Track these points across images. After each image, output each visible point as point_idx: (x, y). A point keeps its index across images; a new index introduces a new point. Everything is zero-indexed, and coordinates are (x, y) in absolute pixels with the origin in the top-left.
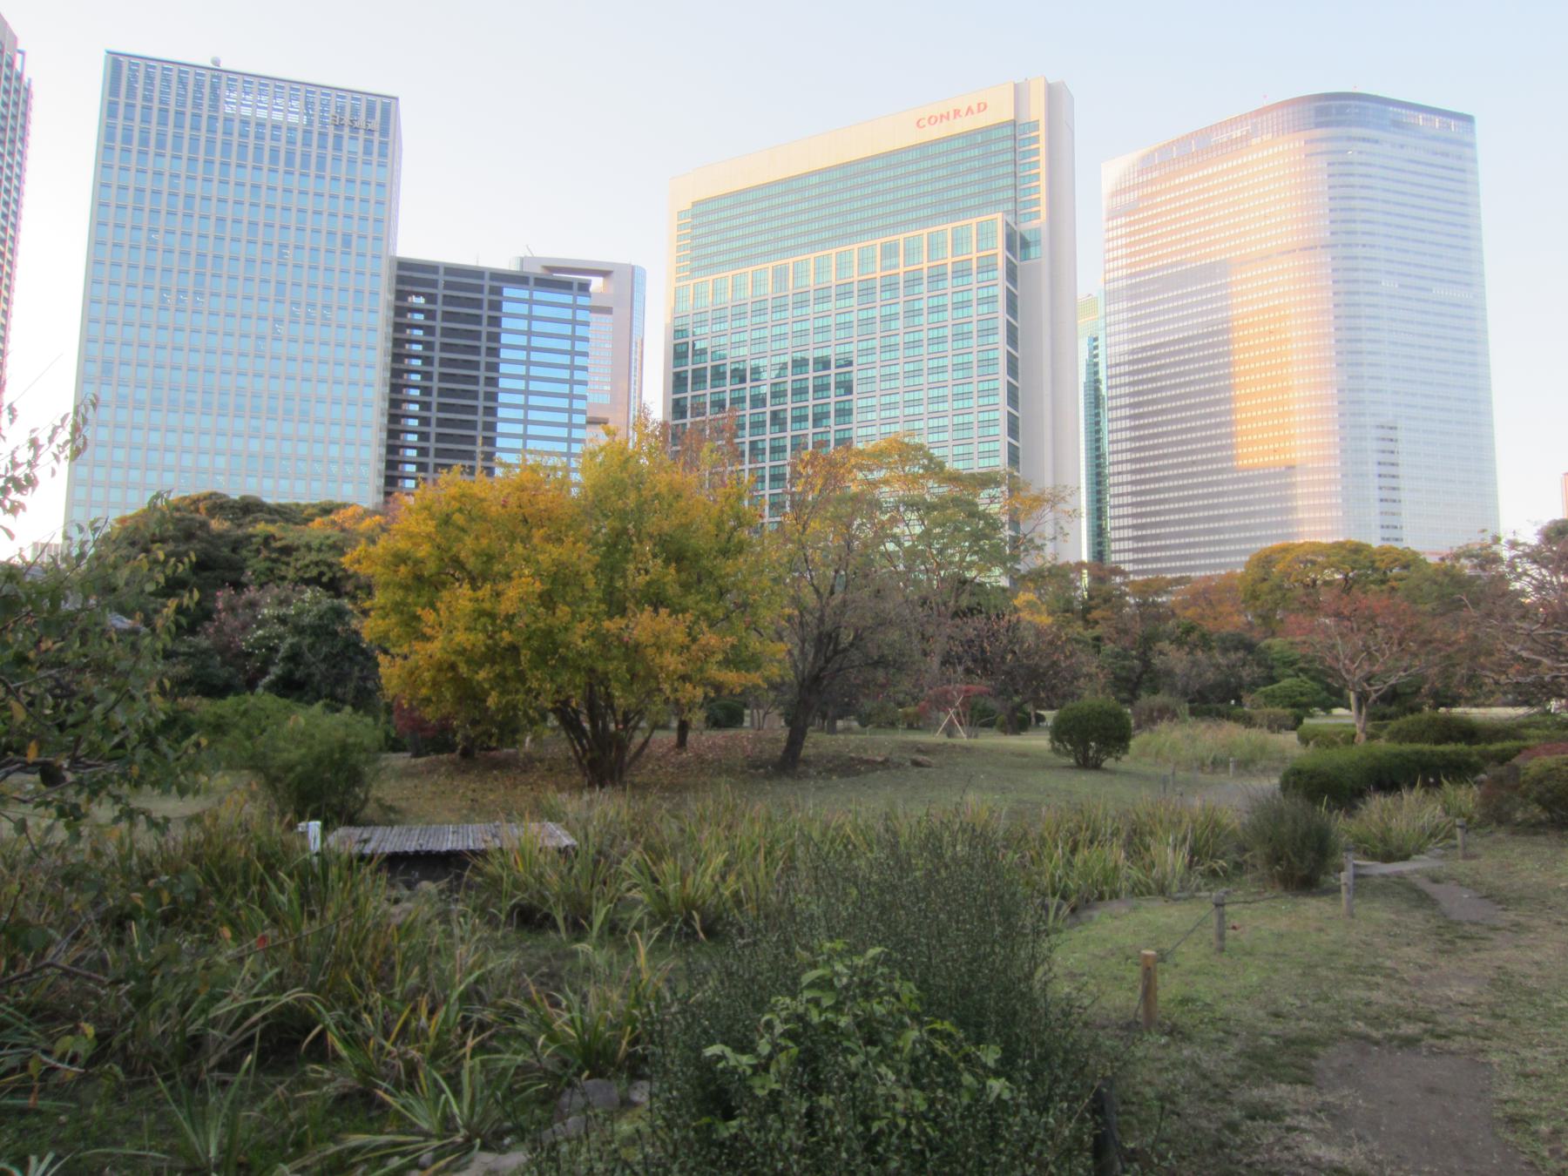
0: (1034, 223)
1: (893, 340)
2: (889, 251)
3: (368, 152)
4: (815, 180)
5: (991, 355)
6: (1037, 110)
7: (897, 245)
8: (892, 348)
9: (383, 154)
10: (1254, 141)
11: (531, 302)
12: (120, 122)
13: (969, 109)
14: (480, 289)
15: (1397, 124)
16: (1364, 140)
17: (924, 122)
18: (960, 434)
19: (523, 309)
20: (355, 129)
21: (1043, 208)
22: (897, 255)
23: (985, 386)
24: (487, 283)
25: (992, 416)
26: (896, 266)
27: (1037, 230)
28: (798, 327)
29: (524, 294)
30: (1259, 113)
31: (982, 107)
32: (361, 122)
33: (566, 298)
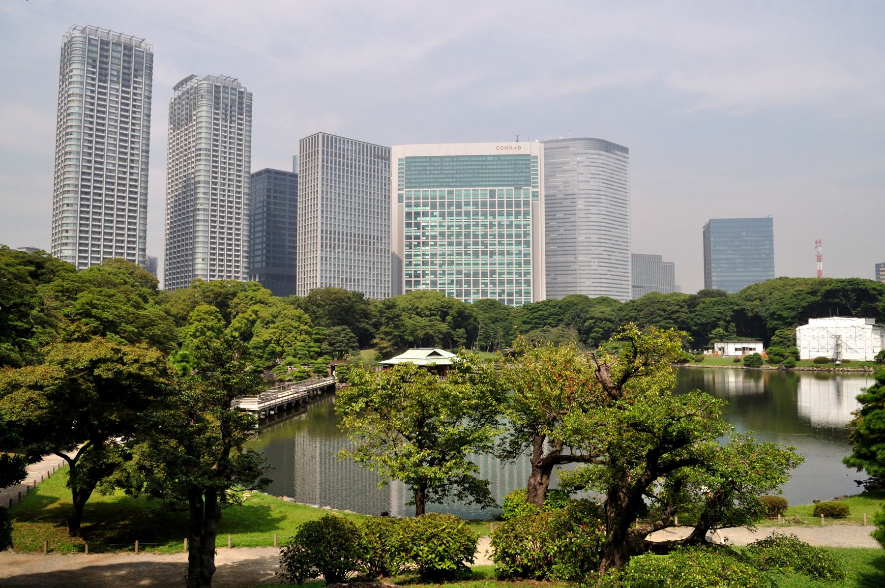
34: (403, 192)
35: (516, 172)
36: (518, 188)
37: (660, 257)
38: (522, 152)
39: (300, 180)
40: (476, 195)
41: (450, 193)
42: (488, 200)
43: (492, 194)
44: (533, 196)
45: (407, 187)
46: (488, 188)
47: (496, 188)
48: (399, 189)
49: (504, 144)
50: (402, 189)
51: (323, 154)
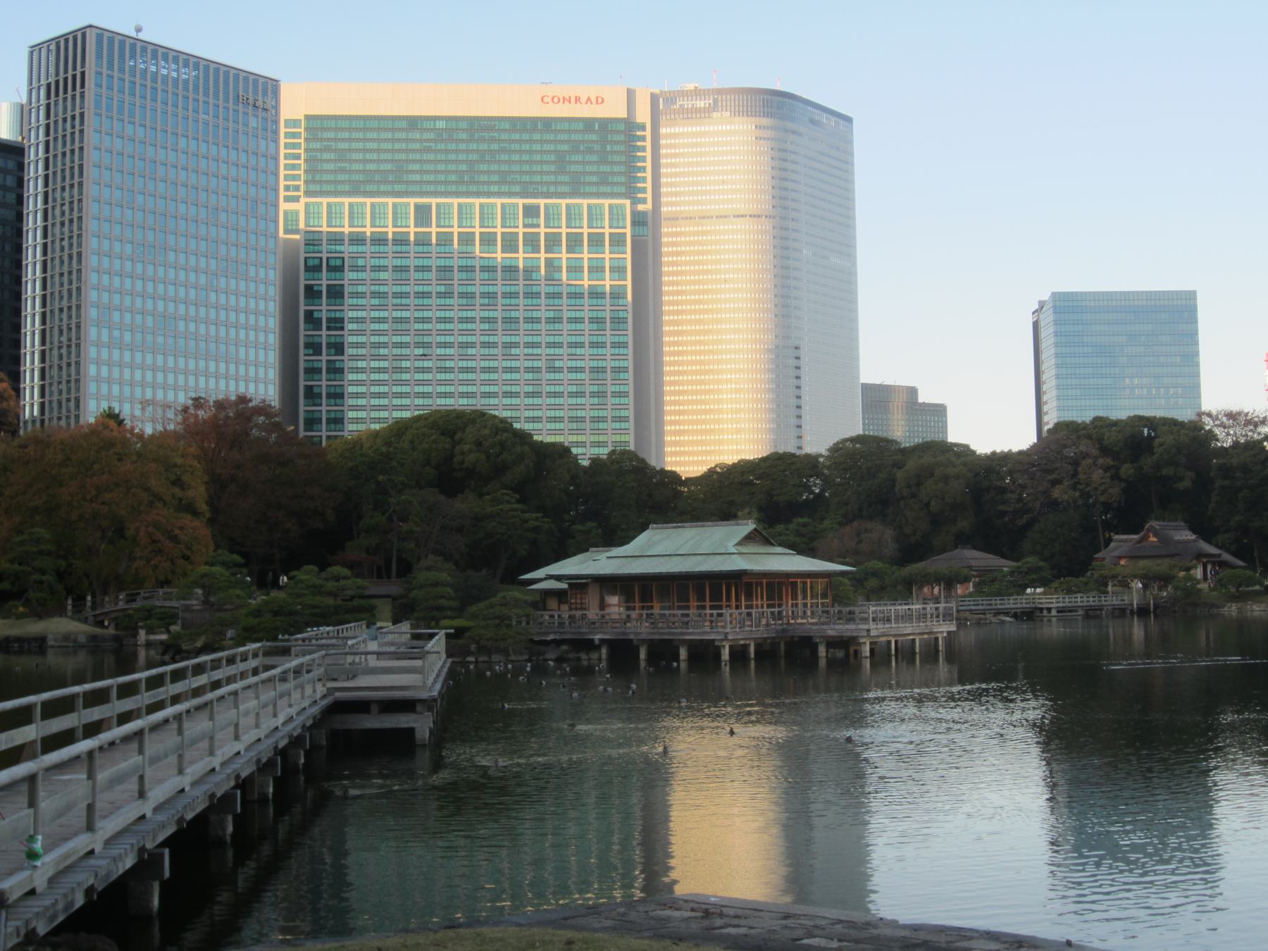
0: (641, 207)
1: (535, 289)
2: (531, 212)
4: (440, 125)
5: (621, 314)
6: (643, 115)
7: (538, 207)
8: (537, 295)
10: (715, 115)
13: (589, 99)
15: (813, 122)
16: (794, 132)
17: (549, 99)
18: (595, 376)
21: (649, 195)
22: (538, 216)
23: (616, 339)
25: (622, 364)
26: (538, 226)
27: (644, 214)
28: (442, 262)
30: (720, 92)
31: (600, 101)
32: (260, 103)
34: (300, 206)
37: (913, 391)
39: (31, 155)
42: (521, 230)
44: (634, 223)
45: (308, 193)
48: (287, 199)
50: (296, 199)
51: (99, 85)
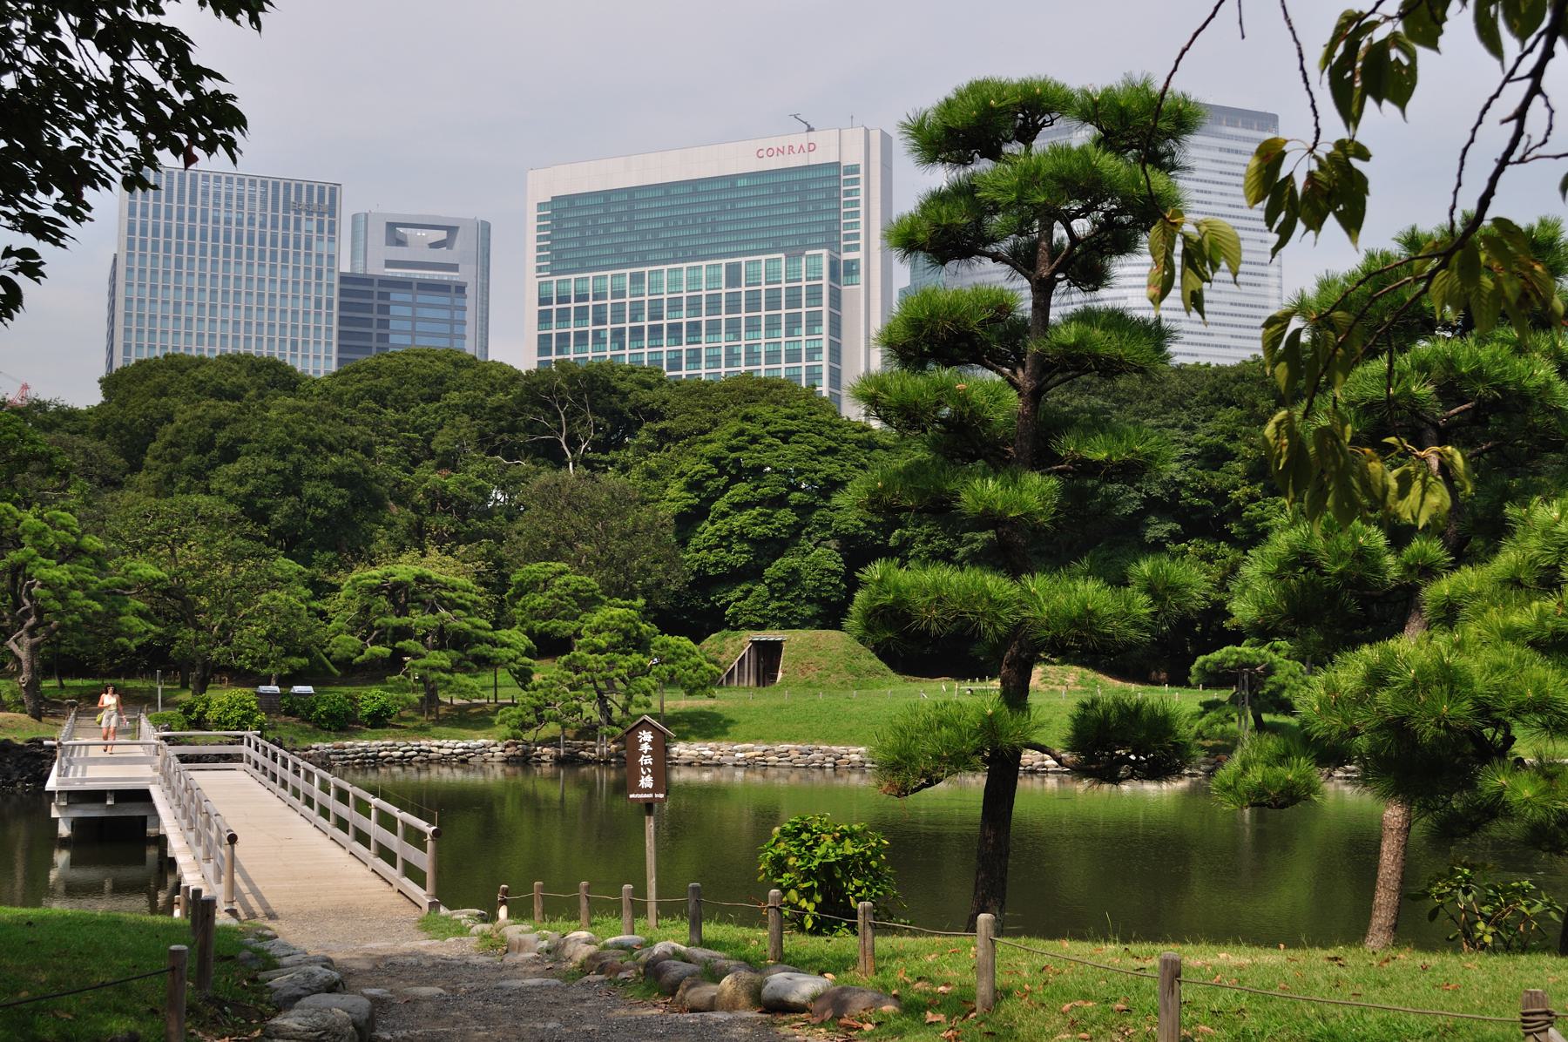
3: (320, 230)
9: (332, 231)
11: (413, 305)
12: (138, 218)
14: (369, 294)
19: (407, 312)
20: (309, 213)
24: (376, 289)
27: (856, 262)
29: (407, 297)
33: (444, 300)
35: (804, 213)
36: (794, 255)
38: (815, 159)
40: (694, 282)
41: (637, 279)
42: (724, 291)
43: (733, 276)
46: (724, 262)
47: (743, 260)
49: (775, 143)
